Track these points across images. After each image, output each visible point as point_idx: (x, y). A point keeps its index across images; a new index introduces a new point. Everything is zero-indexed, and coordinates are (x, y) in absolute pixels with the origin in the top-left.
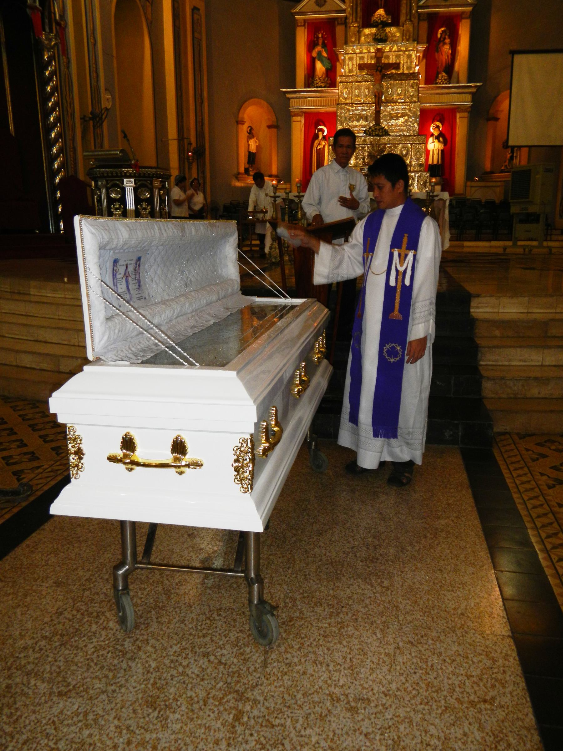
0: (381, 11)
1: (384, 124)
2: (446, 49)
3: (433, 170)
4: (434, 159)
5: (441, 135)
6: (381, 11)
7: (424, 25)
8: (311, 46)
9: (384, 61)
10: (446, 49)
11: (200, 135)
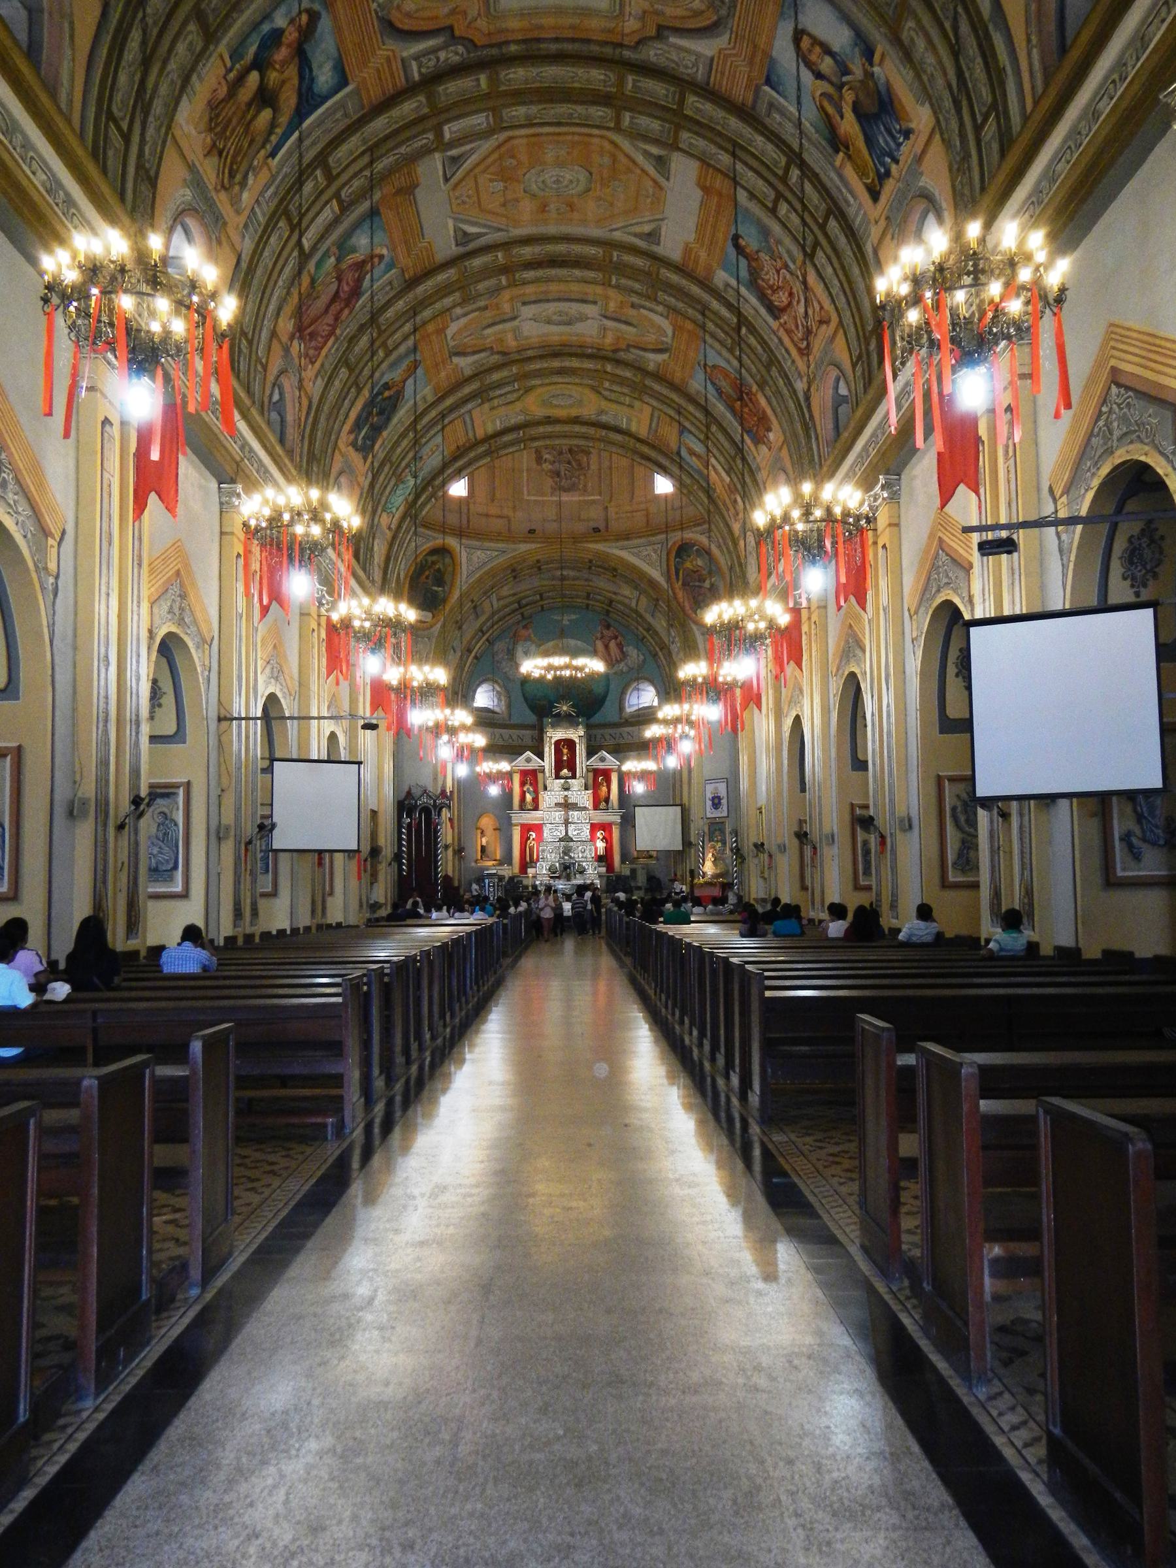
0: (565, 771)
1: (570, 834)
2: (604, 789)
3: (599, 859)
4: (601, 852)
5: (604, 838)
6: (565, 771)
7: (591, 775)
8: (523, 784)
9: (570, 801)
10: (604, 789)
11: (459, 839)
